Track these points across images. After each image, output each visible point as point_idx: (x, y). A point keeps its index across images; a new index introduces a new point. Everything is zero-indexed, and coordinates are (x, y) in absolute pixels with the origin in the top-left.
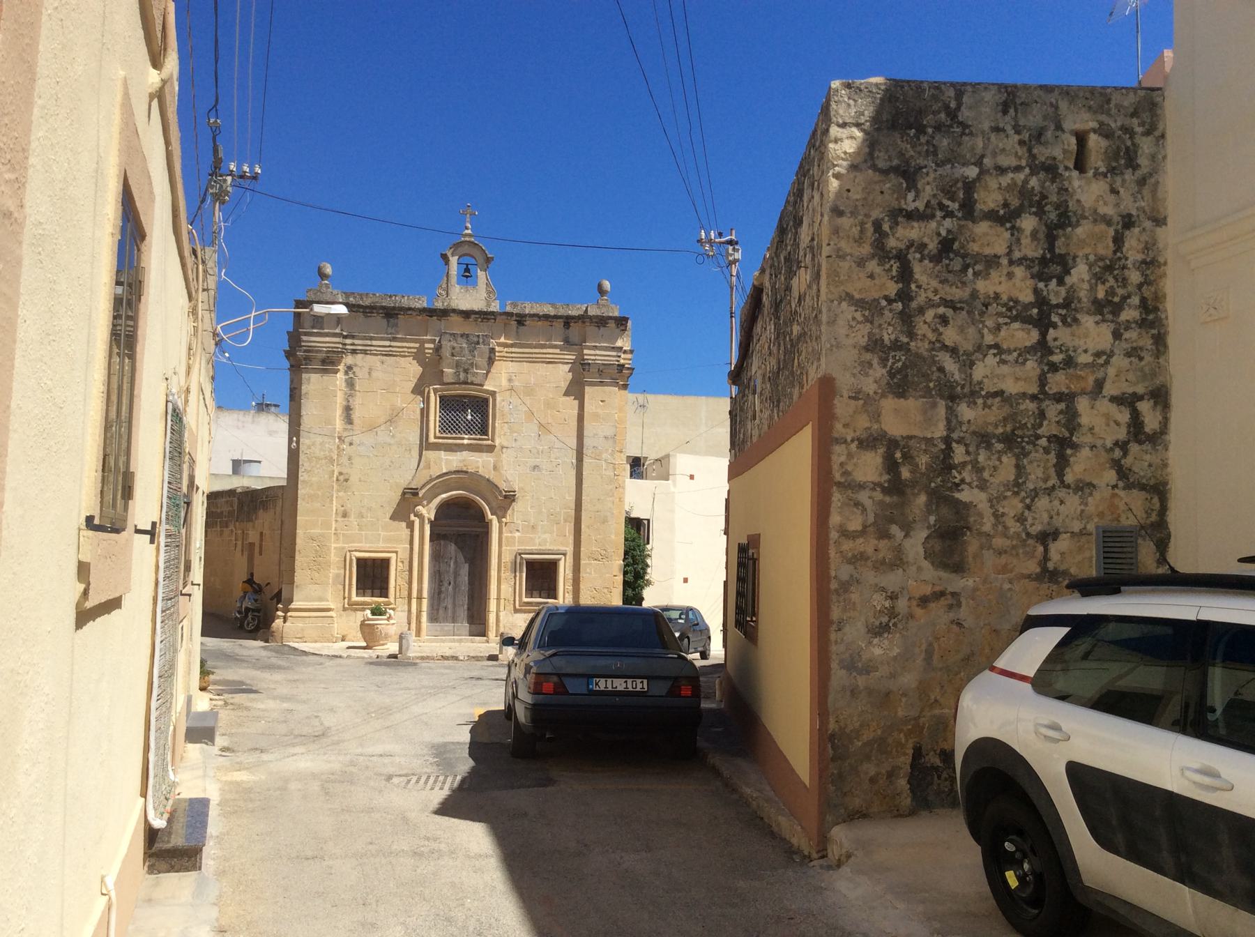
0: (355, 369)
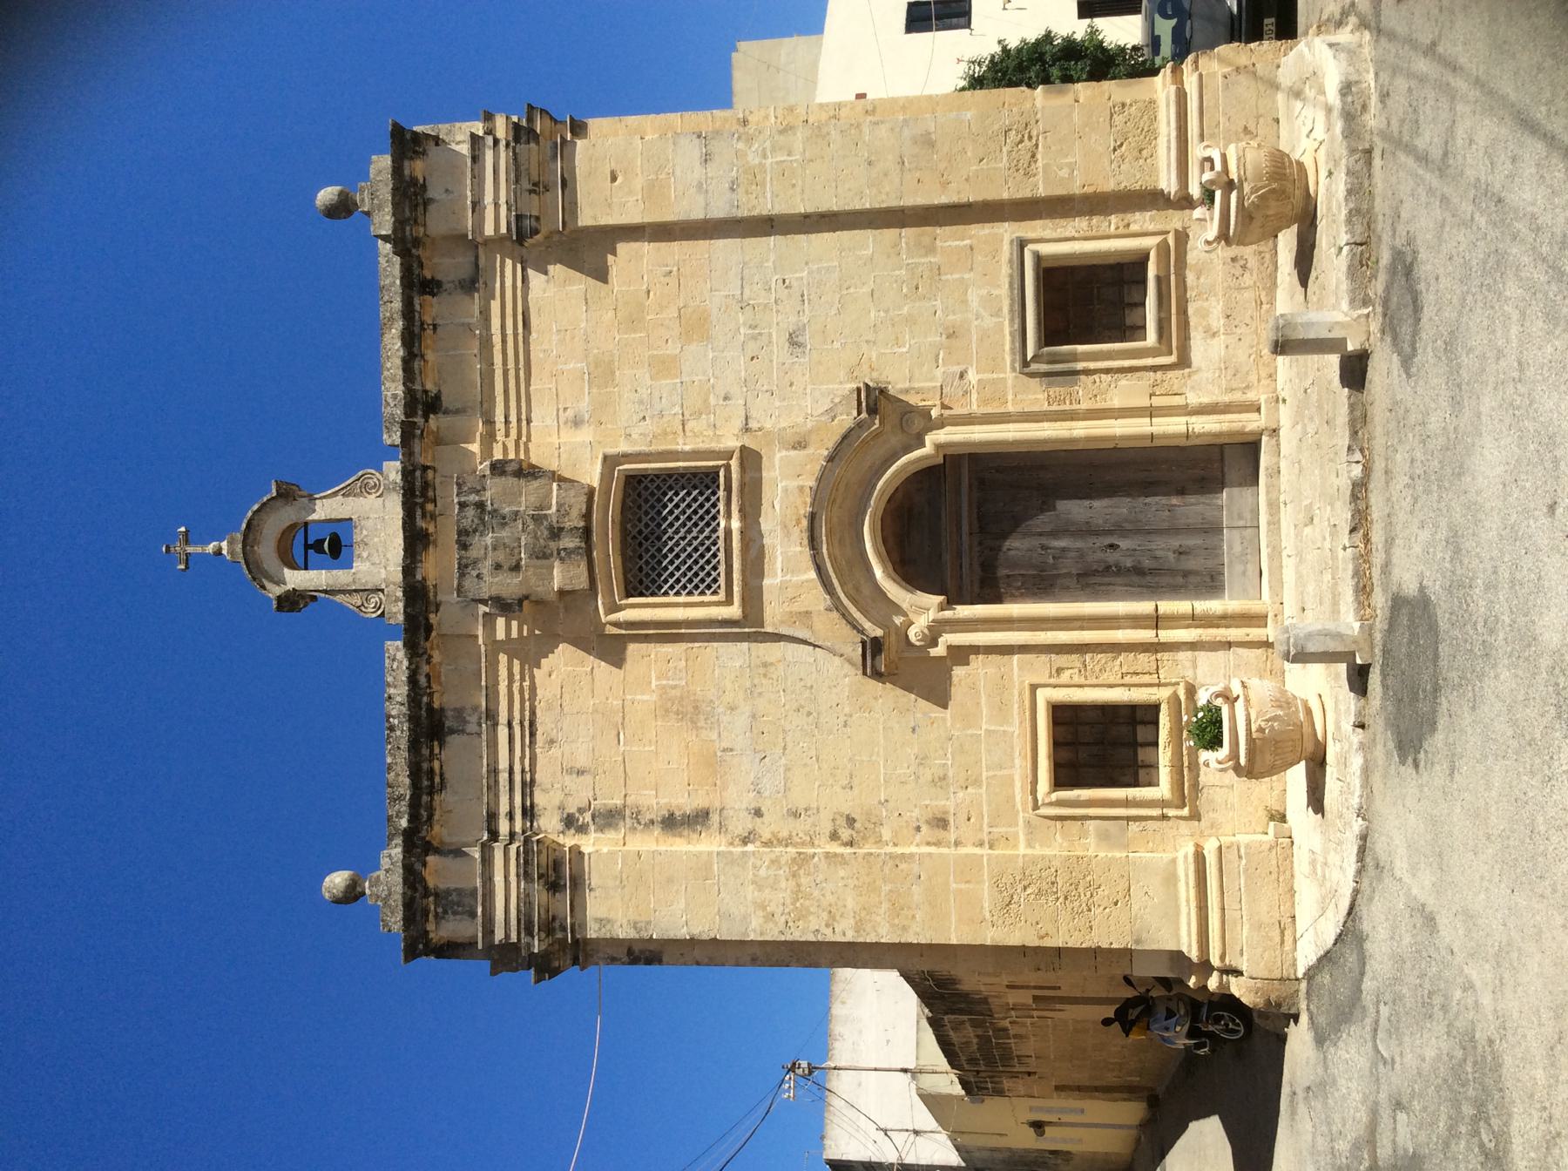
0: (573, 810)
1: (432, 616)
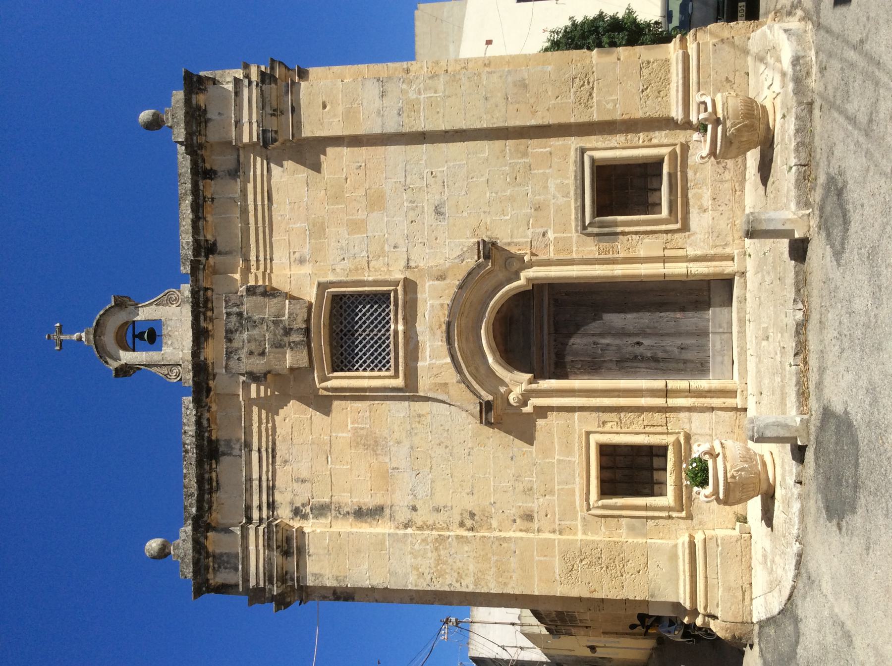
0: (299, 505)
1: (211, 382)
